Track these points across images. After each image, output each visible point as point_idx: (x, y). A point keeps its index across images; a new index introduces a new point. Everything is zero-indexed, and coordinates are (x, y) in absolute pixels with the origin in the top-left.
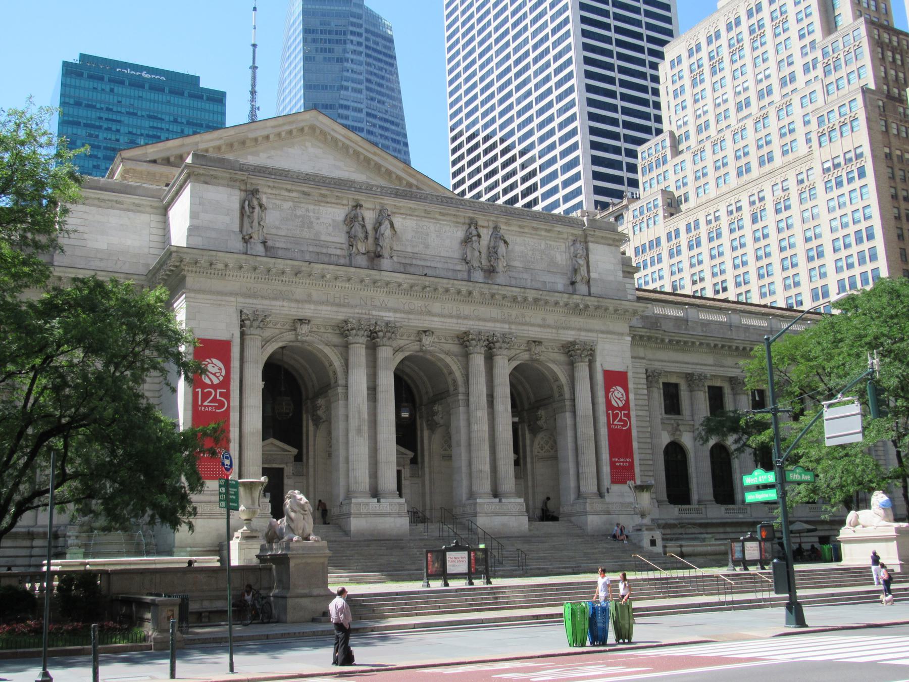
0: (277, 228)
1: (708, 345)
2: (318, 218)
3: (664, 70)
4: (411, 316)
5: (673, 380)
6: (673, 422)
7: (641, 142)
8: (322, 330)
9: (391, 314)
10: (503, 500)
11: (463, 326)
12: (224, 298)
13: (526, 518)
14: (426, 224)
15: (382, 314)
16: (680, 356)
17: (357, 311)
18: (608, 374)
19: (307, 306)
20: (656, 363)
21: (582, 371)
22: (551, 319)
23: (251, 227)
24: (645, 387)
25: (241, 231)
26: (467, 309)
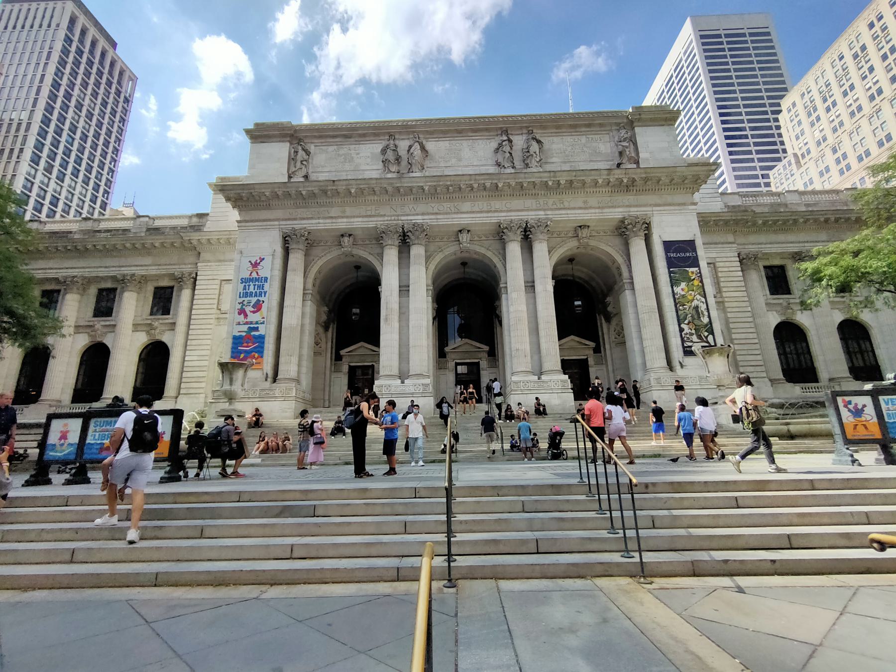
0: (323, 167)
1: (816, 220)
2: (358, 154)
3: (783, 118)
4: (439, 217)
5: (777, 262)
6: (781, 301)
7: (771, 168)
8: (368, 242)
9: (420, 217)
10: (543, 377)
11: (493, 218)
12: (269, 223)
13: (572, 395)
14: (459, 142)
15: (410, 218)
16: (781, 237)
17: (386, 218)
18: (668, 246)
19: (340, 220)
20: (750, 246)
21: (638, 246)
22: (593, 201)
23: (295, 167)
24: (739, 269)
25: (288, 172)
26: (497, 204)
